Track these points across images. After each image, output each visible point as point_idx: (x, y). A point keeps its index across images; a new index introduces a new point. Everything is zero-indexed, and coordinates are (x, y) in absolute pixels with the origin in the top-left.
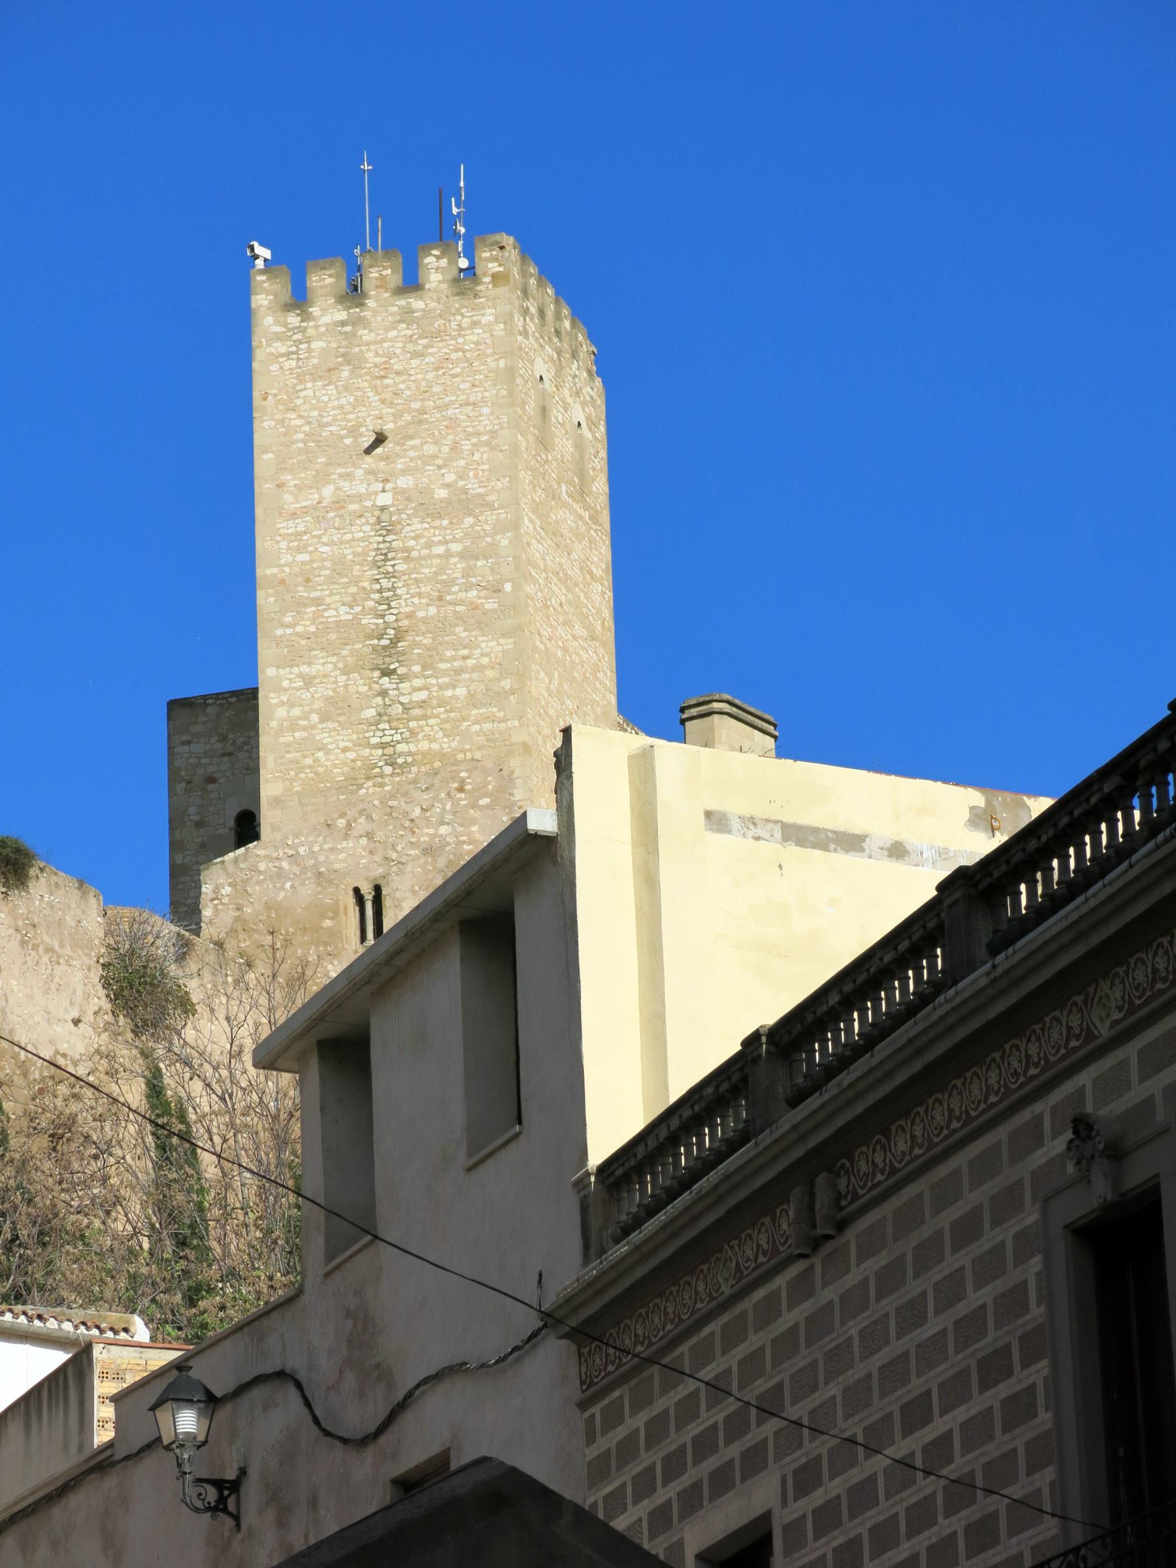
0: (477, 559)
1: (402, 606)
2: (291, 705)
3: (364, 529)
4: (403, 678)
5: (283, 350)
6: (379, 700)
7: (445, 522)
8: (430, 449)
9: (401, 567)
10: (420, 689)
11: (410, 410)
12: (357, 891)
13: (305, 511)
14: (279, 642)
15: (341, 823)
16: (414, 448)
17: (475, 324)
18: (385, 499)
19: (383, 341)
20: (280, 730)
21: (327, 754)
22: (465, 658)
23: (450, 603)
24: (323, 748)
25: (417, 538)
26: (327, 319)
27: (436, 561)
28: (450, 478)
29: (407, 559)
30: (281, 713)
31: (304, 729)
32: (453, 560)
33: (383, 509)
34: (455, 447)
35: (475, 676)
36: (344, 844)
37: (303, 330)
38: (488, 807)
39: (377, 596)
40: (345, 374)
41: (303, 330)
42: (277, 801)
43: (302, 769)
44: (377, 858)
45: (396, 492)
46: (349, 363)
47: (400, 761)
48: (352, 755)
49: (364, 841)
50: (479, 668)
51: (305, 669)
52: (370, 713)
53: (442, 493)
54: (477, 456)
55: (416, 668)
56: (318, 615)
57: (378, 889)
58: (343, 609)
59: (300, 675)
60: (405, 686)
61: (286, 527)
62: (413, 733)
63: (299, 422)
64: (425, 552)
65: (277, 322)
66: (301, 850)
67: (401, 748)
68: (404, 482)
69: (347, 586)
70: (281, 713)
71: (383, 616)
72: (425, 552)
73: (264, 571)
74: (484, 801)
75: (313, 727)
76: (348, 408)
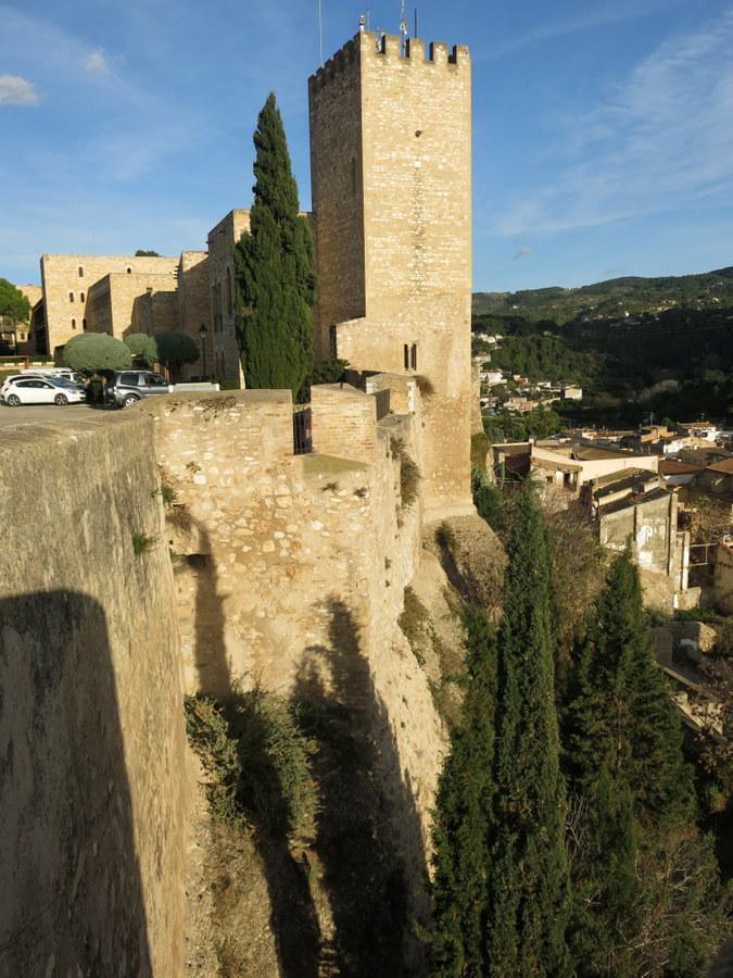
0: (455, 201)
1: (426, 215)
2: (378, 255)
3: (408, 177)
4: (424, 251)
6: (414, 260)
8: (436, 144)
9: (424, 199)
10: (429, 257)
11: (429, 123)
12: (406, 346)
15: (400, 315)
17: (456, 88)
18: (418, 164)
19: (418, 85)
24: (392, 278)
26: (394, 67)
28: (444, 160)
32: (445, 200)
33: (417, 169)
34: (447, 145)
37: (384, 70)
38: (458, 315)
40: (402, 97)
41: (384, 70)
42: (372, 300)
45: (423, 162)
46: (403, 92)
48: (403, 283)
50: (454, 252)
51: (384, 239)
52: (411, 265)
53: (441, 167)
57: (415, 346)
58: (400, 214)
59: (382, 242)
61: (377, 169)
62: (428, 277)
63: (381, 116)
66: (384, 325)
67: (423, 283)
68: (426, 158)
70: (374, 259)
73: (367, 188)
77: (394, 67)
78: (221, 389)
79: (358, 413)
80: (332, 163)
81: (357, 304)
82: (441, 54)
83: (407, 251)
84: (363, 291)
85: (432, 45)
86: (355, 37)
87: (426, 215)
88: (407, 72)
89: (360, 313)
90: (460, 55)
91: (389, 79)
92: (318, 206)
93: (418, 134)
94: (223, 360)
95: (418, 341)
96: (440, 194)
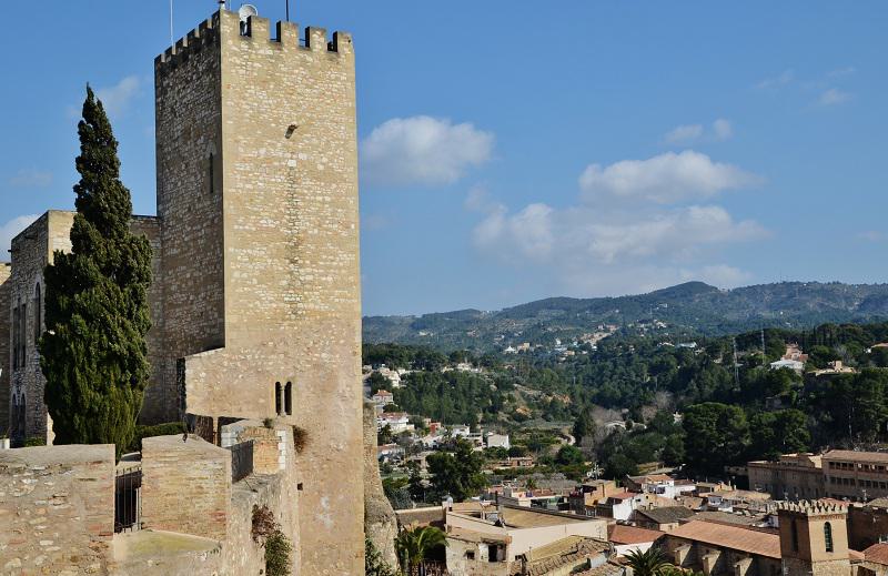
1: (305, 224)
3: (280, 178)
4: (301, 266)
5: (238, 62)
8: (315, 141)
12: (278, 384)
13: (251, 160)
14: (236, 232)
17: (337, 79)
18: (292, 163)
20: (236, 285)
21: (261, 303)
22: (332, 261)
23: (327, 230)
24: (259, 299)
25: (309, 189)
26: (261, 52)
27: (318, 205)
28: (325, 160)
29: (303, 200)
30: (236, 274)
31: (249, 286)
33: (291, 168)
35: (337, 271)
37: (250, 54)
38: (344, 345)
39: (288, 217)
41: (250, 54)
42: (234, 326)
43: (248, 309)
45: (298, 161)
47: (300, 312)
48: (275, 306)
49: (282, 356)
50: (340, 268)
51: (249, 251)
52: (284, 283)
53: (321, 167)
54: (338, 152)
55: (308, 262)
57: (289, 385)
58: (270, 221)
59: (247, 254)
60: (302, 271)
63: (246, 107)
64: (312, 198)
65: (234, 44)
68: (302, 156)
69: (273, 208)
70: (236, 274)
72: (312, 198)
74: (342, 341)
75: (254, 286)
76: (273, 107)
77: (261, 52)
78: (13, 446)
79: (205, 474)
80: (184, 159)
81: (213, 330)
82: (320, 43)
83: (279, 266)
84: (221, 314)
85: (307, 30)
86: (214, 16)
87: (305, 224)
88: (278, 58)
89: (220, 344)
90: (341, 42)
91: (256, 65)
92: (165, 210)
93: (291, 129)
94: (23, 407)
95: (293, 378)
96: (320, 198)
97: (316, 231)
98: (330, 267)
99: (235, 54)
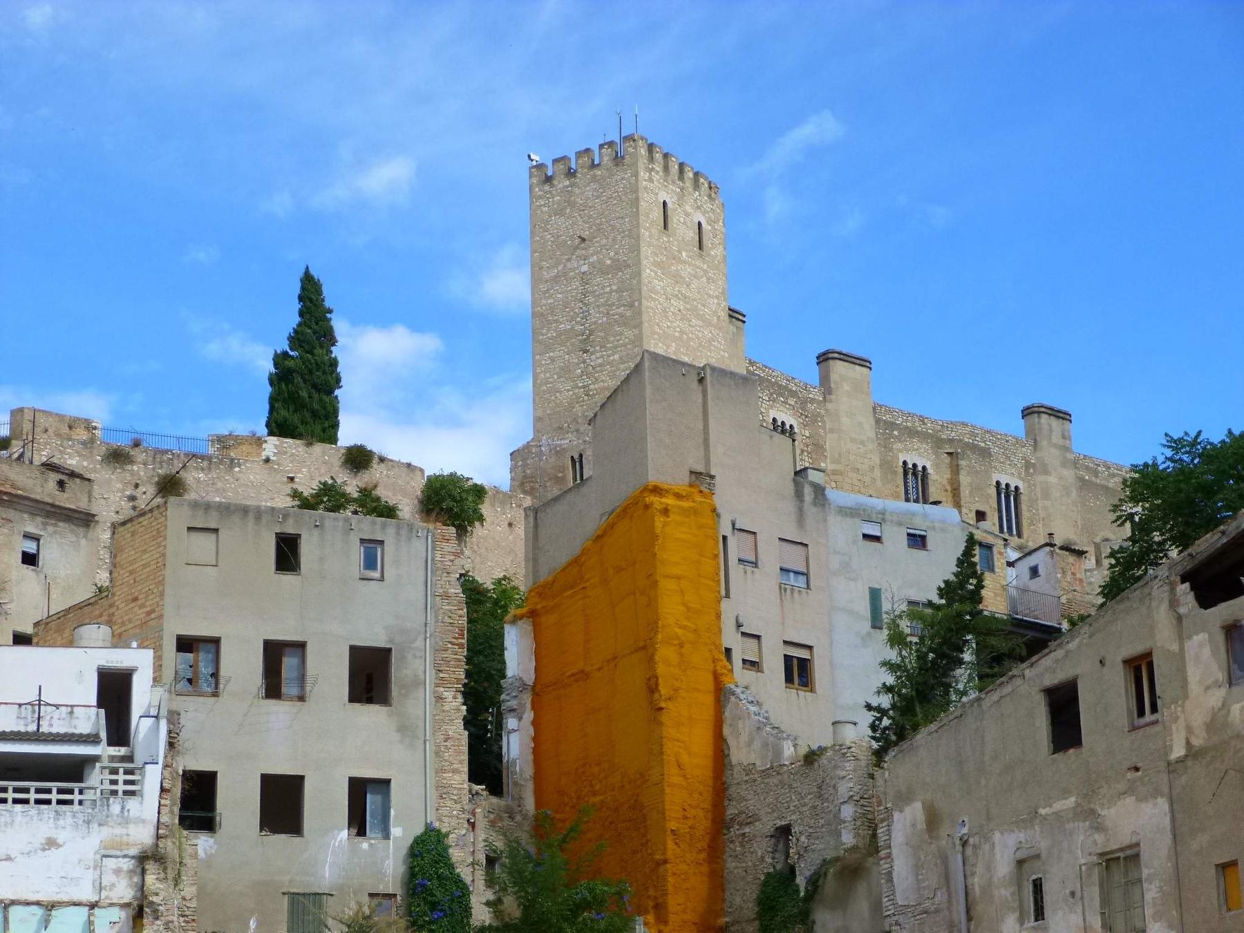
0: (623, 292)
4: (592, 354)
5: (542, 203)
7: (610, 276)
10: (597, 358)
12: (572, 457)
16: (597, 242)
17: (623, 179)
18: (585, 268)
22: (618, 341)
24: (560, 392)
26: (561, 186)
27: (606, 295)
33: (584, 273)
36: (567, 436)
40: (568, 210)
41: (550, 192)
44: (581, 441)
51: (552, 354)
53: (608, 262)
54: (623, 243)
55: (598, 348)
56: (557, 327)
57: (581, 456)
59: (550, 358)
65: (540, 190)
67: (592, 387)
71: (583, 325)
76: (569, 227)
95: (583, 450)
97: (605, 319)
98: (616, 347)
99: (540, 197)
